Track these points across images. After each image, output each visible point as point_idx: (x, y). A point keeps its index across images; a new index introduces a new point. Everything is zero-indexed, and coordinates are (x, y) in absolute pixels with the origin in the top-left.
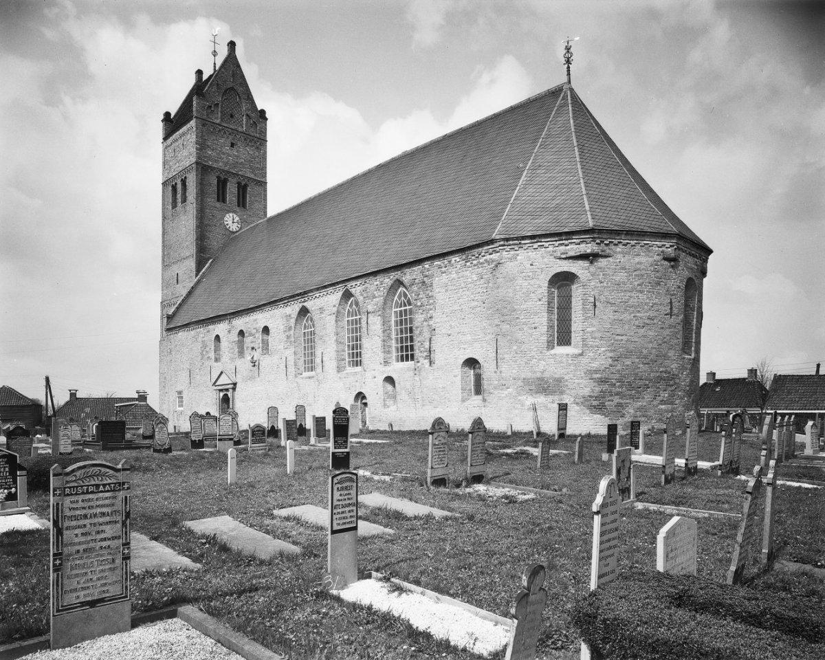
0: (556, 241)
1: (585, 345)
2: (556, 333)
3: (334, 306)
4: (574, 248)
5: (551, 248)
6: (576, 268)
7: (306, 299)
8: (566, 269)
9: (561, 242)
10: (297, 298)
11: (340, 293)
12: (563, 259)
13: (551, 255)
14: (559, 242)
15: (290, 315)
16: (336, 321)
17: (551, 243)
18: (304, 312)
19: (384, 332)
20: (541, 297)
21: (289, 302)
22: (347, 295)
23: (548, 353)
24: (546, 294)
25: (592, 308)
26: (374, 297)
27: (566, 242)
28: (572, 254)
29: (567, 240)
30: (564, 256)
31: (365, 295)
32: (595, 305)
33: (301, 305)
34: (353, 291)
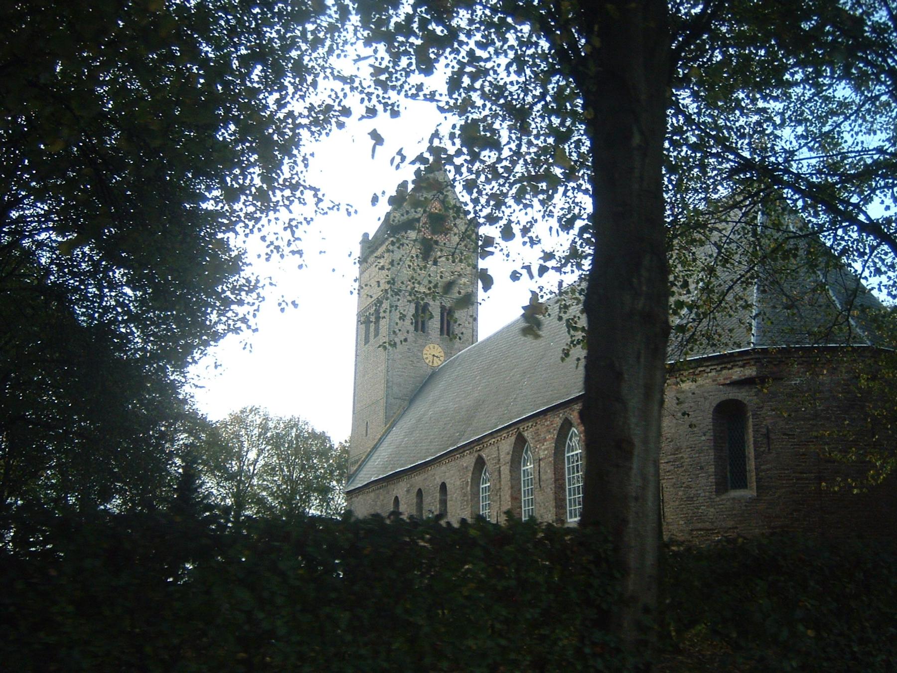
0: (718, 365)
1: (759, 488)
2: (728, 474)
3: (508, 454)
4: (737, 373)
5: (713, 373)
6: (742, 395)
7: (481, 446)
8: (731, 396)
9: (723, 366)
10: (472, 446)
11: (513, 439)
12: (728, 384)
13: (714, 381)
14: (721, 366)
15: (467, 467)
16: (510, 472)
17: (712, 367)
18: (480, 463)
19: (556, 480)
20: (705, 430)
21: (464, 451)
22: (521, 441)
23: (718, 499)
24: (711, 427)
25: (765, 441)
26: (545, 440)
27: (729, 366)
28: (735, 377)
29: (728, 363)
30: (729, 382)
31: (537, 439)
32: (768, 438)
33: (476, 455)
34: (525, 434)
